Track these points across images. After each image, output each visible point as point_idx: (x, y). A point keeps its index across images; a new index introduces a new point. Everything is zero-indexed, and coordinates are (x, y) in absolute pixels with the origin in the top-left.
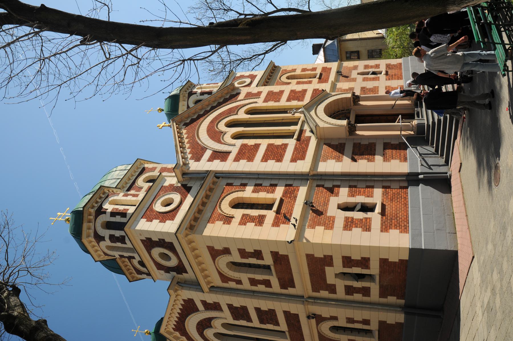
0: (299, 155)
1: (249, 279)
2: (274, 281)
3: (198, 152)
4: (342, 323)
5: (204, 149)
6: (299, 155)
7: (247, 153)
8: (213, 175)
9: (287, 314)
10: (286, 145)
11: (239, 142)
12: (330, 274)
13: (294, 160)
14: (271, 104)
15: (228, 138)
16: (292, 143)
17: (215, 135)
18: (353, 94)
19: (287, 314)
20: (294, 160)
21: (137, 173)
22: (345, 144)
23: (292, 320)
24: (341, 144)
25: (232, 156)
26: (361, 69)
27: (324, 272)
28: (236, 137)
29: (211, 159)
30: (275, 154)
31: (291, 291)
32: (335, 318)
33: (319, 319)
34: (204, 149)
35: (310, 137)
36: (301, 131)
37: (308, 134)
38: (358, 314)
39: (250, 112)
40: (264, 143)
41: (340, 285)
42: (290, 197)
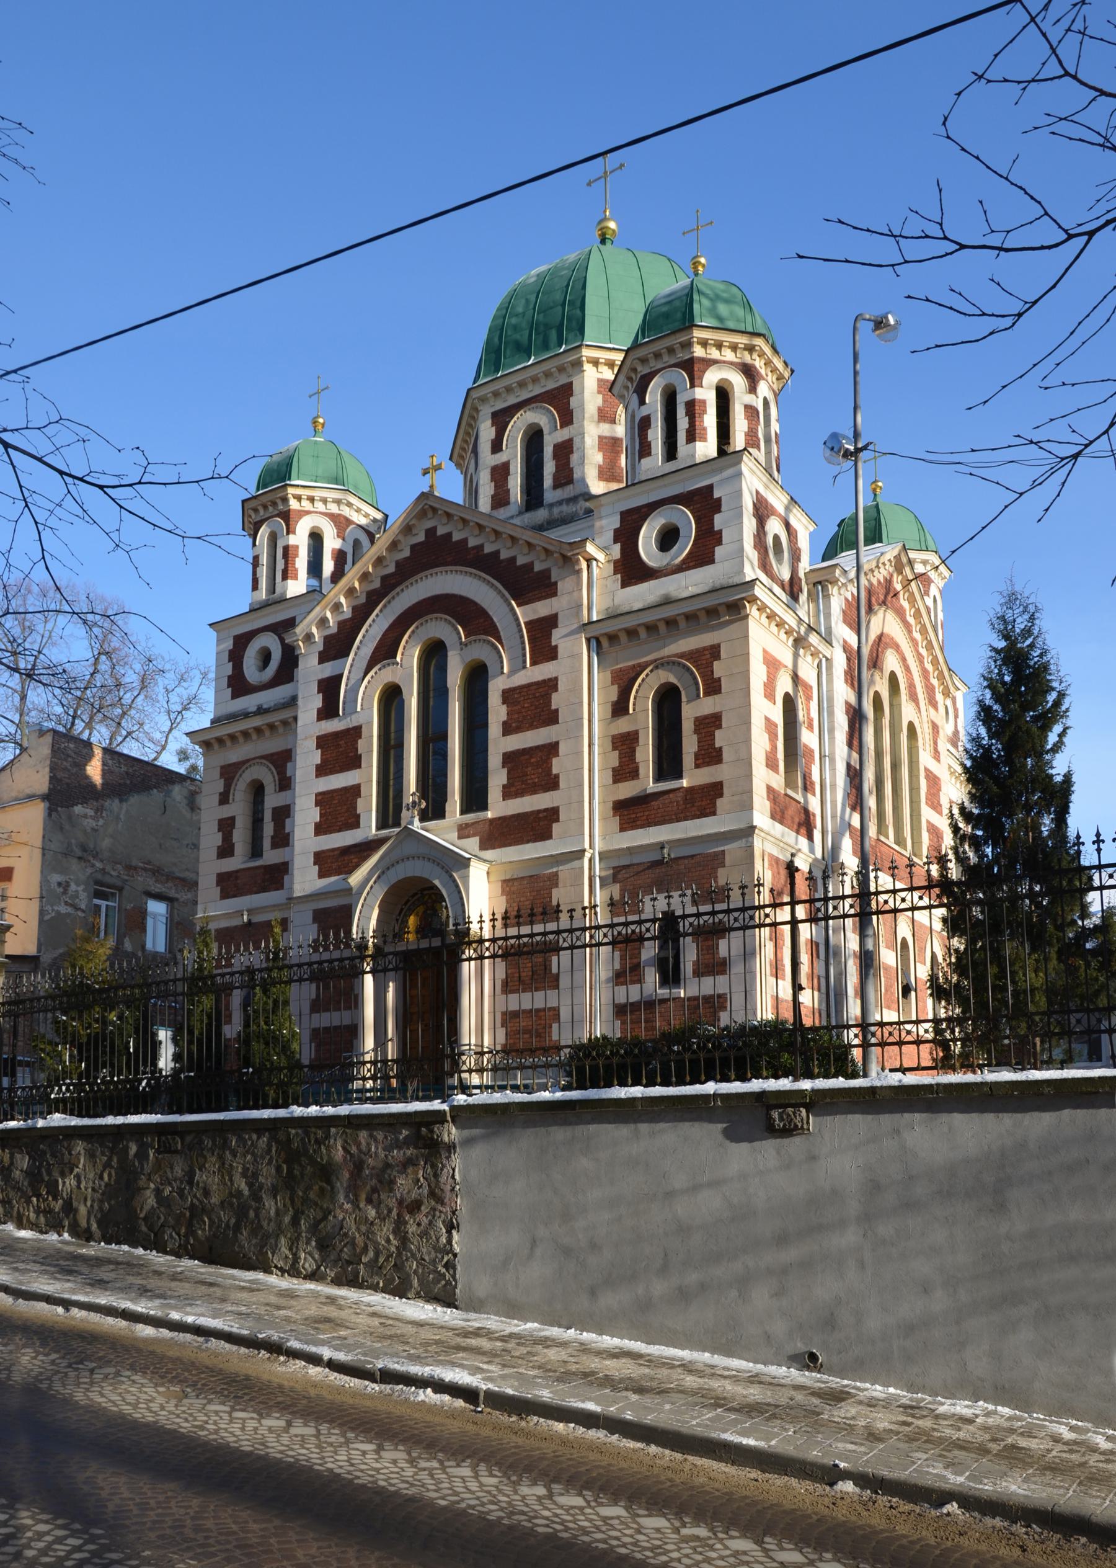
3: (337, 646)
7: (340, 751)
15: (384, 675)
21: (537, 390)
28: (392, 696)
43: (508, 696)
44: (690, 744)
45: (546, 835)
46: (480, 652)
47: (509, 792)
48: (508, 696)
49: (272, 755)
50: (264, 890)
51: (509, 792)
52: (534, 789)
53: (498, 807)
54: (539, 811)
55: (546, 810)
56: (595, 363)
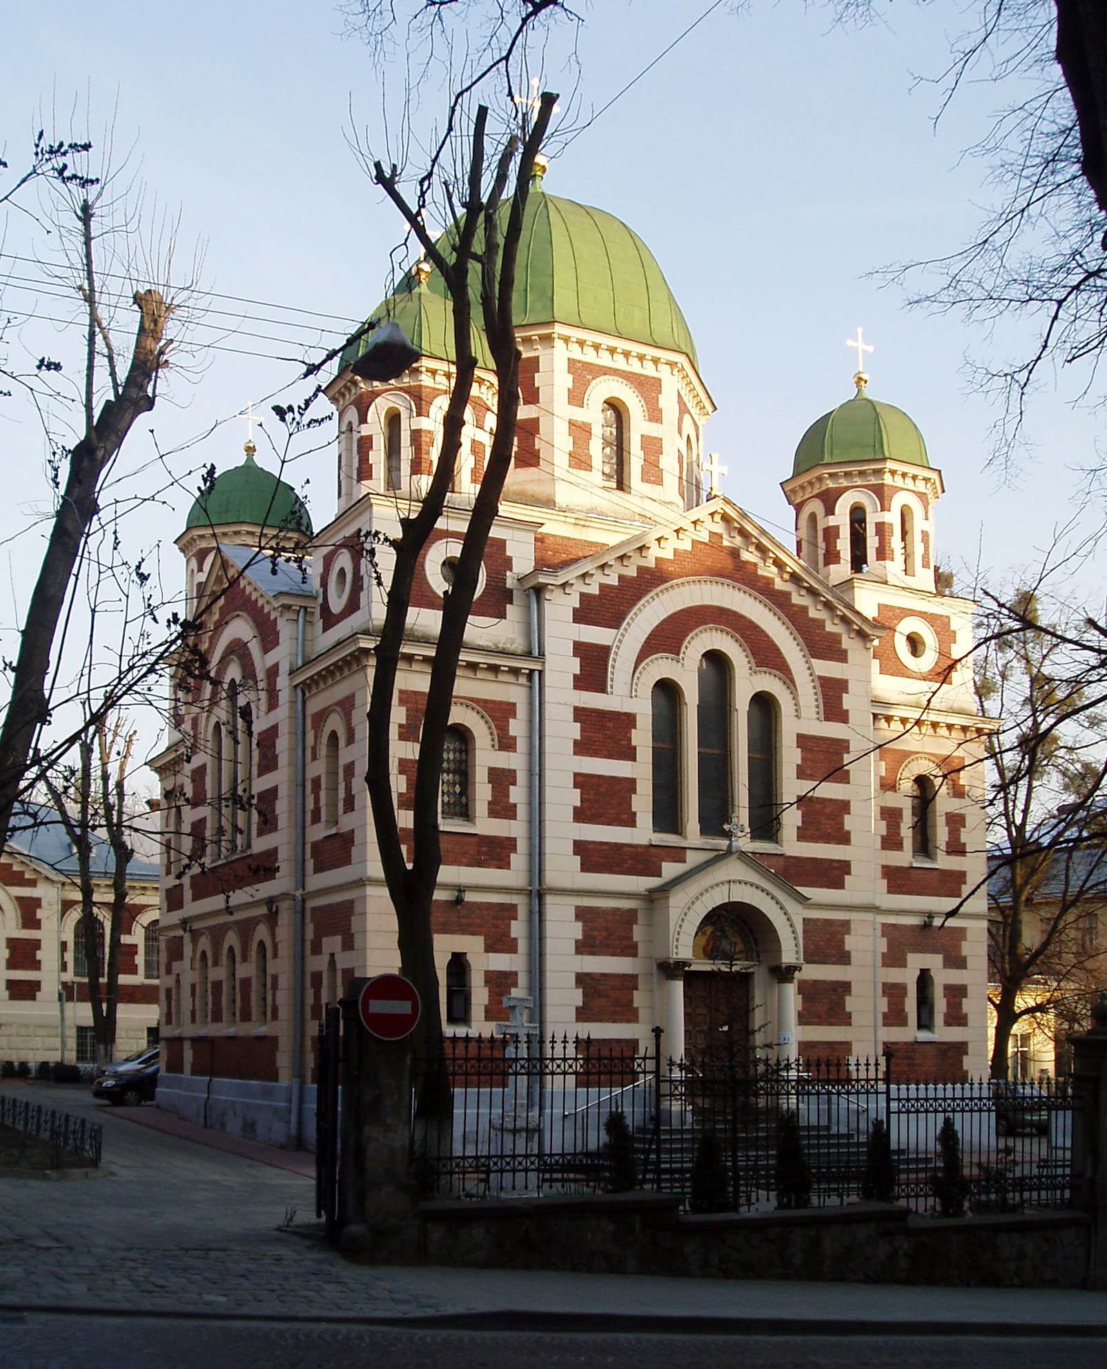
0: (593, 857)
1: (319, 777)
2: (317, 833)
4: (271, 968)
5: (615, 621)
6: (593, 857)
7: (605, 732)
8: (532, 667)
9: (273, 853)
10: (629, 820)
11: (643, 708)
12: (332, 943)
13: (580, 847)
14: (790, 757)
15: (661, 667)
16: (643, 833)
17: (667, 638)
18: (796, 968)
19: (273, 853)
20: (580, 847)
22: (635, 955)
23: (264, 867)
24: (635, 946)
25: (592, 700)
26: (942, 977)
27: (335, 934)
28: (667, 691)
29: (581, 649)
30: (602, 800)
31: (310, 864)
32: (275, 955)
33: (272, 918)
34: (615, 621)
35: (660, 876)
36: (677, 854)
37: (670, 870)
38: (284, 998)
39: (764, 704)
40: (640, 770)
41: (318, 963)
42: (479, 853)
43: (803, 741)
44: (942, 835)
45: (839, 885)
46: (769, 683)
47: (803, 835)
48: (803, 741)
49: (486, 701)
50: (479, 864)
51: (804, 834)
52: (827, 838)
53: (791, 845)
54: (832, 861)
55: (839, 861)
56: (566, 340)
